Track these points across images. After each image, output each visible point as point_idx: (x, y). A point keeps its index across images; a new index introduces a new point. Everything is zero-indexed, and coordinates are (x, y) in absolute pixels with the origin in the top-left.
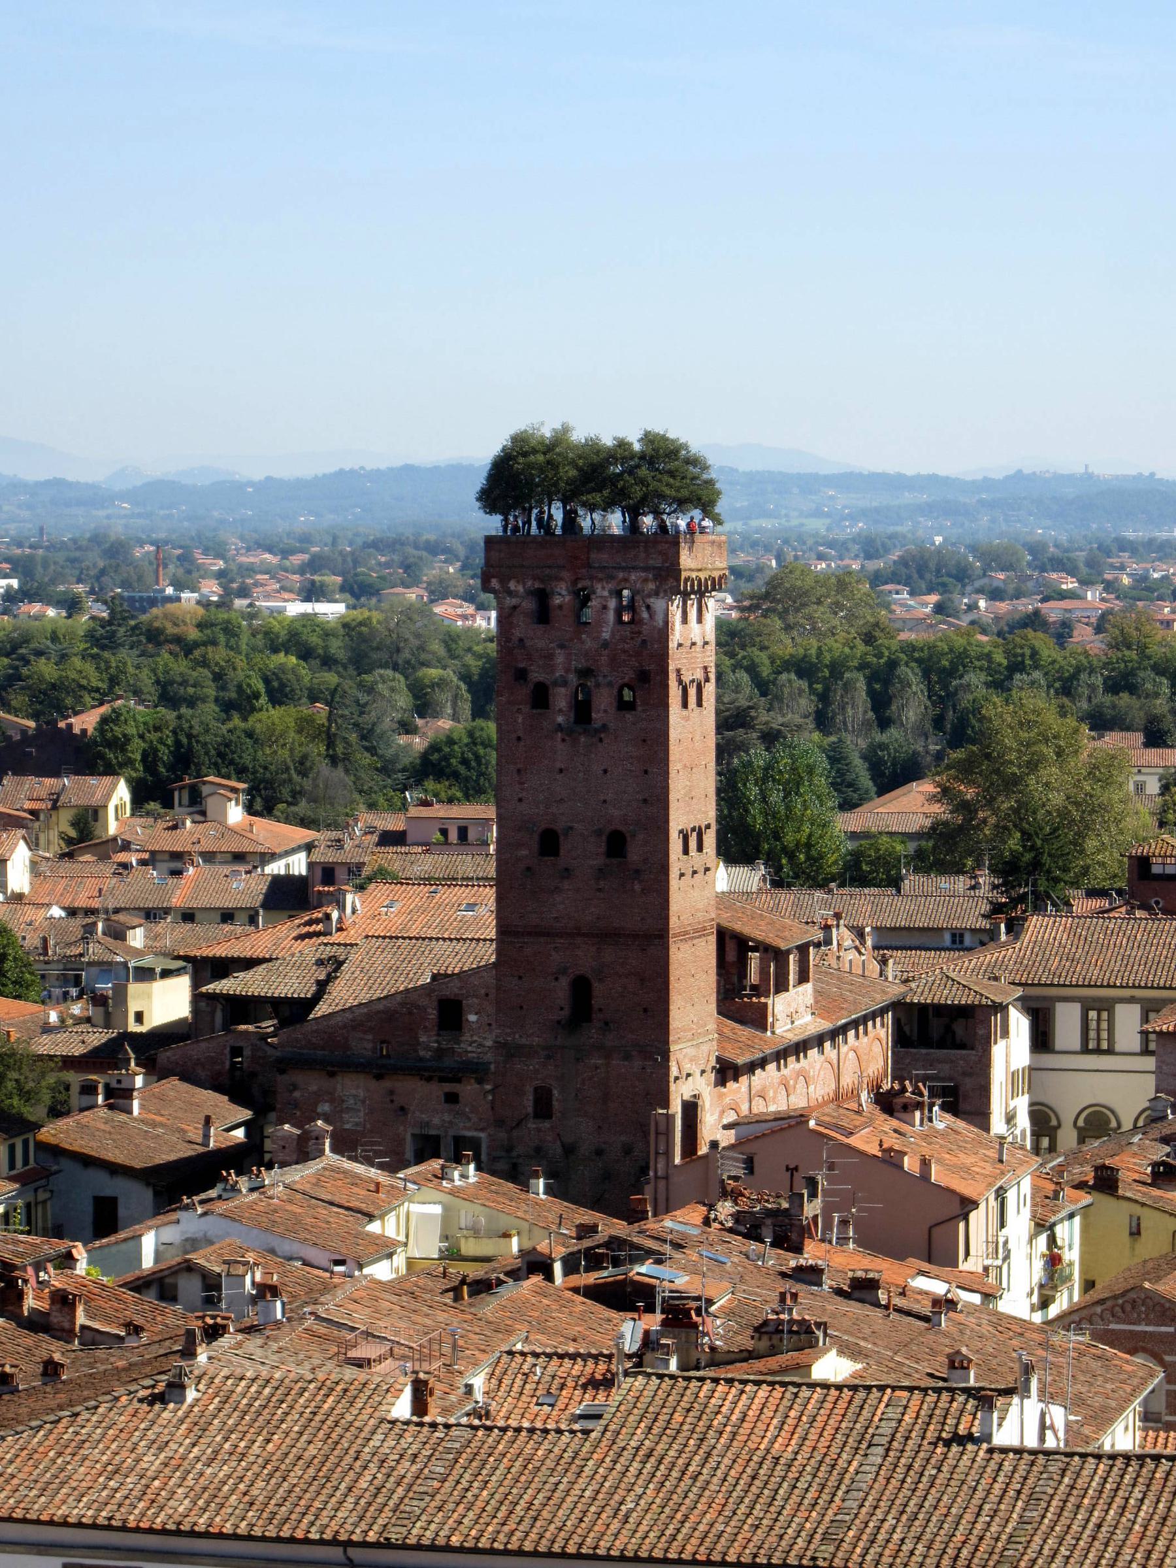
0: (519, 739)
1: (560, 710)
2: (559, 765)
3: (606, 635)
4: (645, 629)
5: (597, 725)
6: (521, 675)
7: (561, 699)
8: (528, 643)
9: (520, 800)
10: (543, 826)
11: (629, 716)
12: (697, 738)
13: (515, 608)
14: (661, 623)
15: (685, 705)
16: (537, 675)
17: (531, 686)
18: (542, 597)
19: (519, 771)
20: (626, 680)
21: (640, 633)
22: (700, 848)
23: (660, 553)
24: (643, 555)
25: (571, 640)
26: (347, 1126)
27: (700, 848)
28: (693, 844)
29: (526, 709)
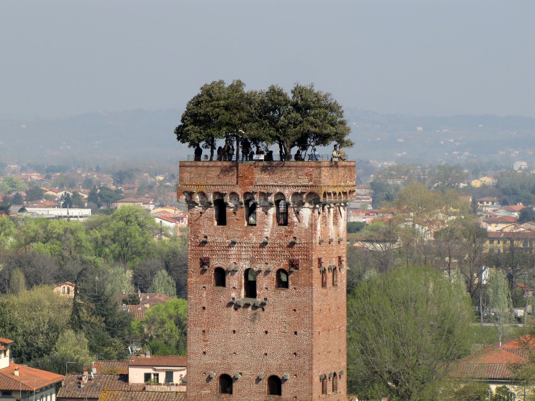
0: (204, 308)
1: (234, 288)
2: (232, 328)
3: (267, 233)
4: (296, 230)
5: (259, 300)
6: (204, 262)
7: (235, 281)
8: (209, 239)
11: (283, 293)
12: (333, 308)
13: (201, 213)
14: (307, 225)
15: (324, 285)
16: (216, 263)
18: (221, 206)
19: (204, 331)
20: (281, 267)
21: (291, 232)
22: (334, 388)
23: (306, 174)
24: (293, 176)
25: (243, 237)
27: (334, 388)
28: (329, 386)
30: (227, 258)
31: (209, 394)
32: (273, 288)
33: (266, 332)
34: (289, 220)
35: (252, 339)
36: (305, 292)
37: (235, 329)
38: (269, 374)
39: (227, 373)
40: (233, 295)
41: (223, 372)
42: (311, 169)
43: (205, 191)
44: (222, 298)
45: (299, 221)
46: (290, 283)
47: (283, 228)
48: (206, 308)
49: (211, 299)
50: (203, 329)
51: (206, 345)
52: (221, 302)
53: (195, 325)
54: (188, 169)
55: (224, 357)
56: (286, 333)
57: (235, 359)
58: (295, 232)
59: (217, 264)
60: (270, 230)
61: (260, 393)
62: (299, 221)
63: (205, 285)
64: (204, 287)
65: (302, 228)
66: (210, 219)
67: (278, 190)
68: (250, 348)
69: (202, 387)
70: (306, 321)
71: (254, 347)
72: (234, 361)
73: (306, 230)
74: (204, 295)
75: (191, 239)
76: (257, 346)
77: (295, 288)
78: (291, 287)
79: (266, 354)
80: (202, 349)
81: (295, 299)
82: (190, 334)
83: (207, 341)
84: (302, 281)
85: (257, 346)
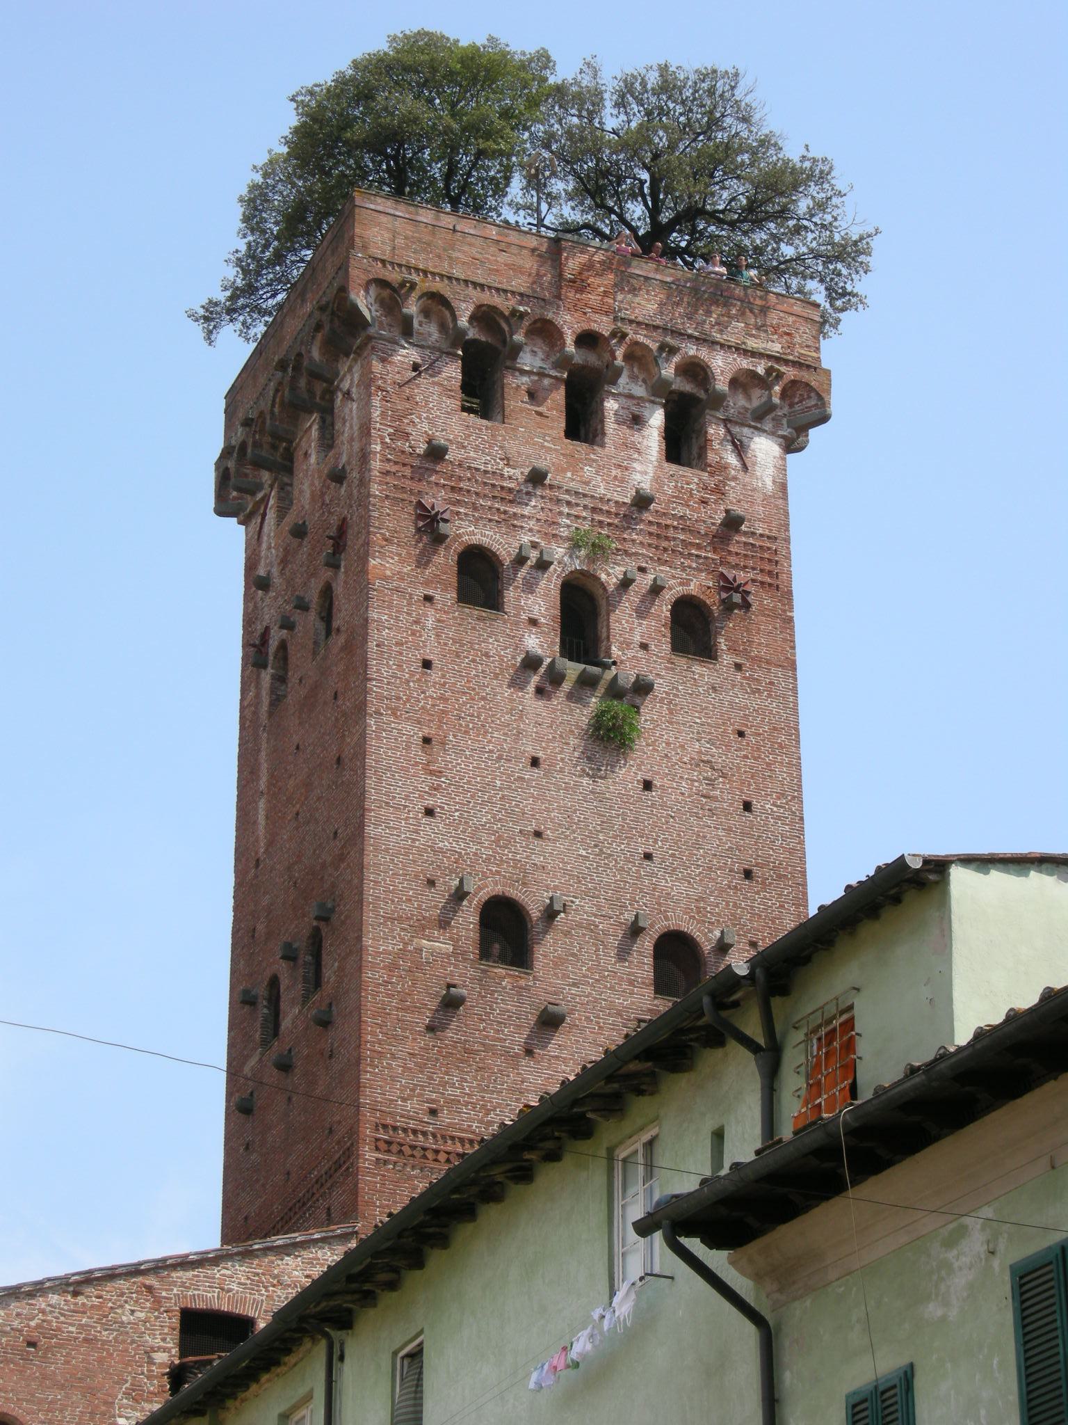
0: (427, 664)
1: (533, 622)
2: (530, 750)
4: (733, 491)
9: (429, 812)
10: (492, 888)
17: (457, 547)
19: (427, 740)
20: (693, 588)
21: (719, 491)
29: (446, 597)
30: (510, 523)
31: (449, 956)
32: (667, 647)
33: (648, 785)
34: (711, 457)
36: (771, 683)
37: (540, 754)
39: (514, 893)
40: (532, 642)
41: (499, 890)
42: (791, 319)
43: (448, 294)
44: (492, 646)
45: (745, 467)
46: (722, 643)
47: (691, 477)
49: (455, 642)
50: (426, 731)
52: (487, 655)
53: (394, 714)
54: (383, 219)
55: (500, 838)
56: (715, 799)
57: (539, 854)
58: (732, 496)
59: (473, 533)
60: (651, 470)
61: (631, 983)
62: (745, 467)
63: (431, 593)
64: (428, 599)
65: (754, 490)
66: (447, 391)
67: (691, 350)
68: (595, 822)
69: (421, 928)
70: (781, 773)
71: (606, 824)
72: (539, 860)
73: (766, 498)
74: (430, 623)
75: (382, 438)
77: (738, 667)
78: (727, 659)
79: (648, 856)
80: (421, 797)
81: (741, 699)
82: (379, 738)
83: (439, 774)
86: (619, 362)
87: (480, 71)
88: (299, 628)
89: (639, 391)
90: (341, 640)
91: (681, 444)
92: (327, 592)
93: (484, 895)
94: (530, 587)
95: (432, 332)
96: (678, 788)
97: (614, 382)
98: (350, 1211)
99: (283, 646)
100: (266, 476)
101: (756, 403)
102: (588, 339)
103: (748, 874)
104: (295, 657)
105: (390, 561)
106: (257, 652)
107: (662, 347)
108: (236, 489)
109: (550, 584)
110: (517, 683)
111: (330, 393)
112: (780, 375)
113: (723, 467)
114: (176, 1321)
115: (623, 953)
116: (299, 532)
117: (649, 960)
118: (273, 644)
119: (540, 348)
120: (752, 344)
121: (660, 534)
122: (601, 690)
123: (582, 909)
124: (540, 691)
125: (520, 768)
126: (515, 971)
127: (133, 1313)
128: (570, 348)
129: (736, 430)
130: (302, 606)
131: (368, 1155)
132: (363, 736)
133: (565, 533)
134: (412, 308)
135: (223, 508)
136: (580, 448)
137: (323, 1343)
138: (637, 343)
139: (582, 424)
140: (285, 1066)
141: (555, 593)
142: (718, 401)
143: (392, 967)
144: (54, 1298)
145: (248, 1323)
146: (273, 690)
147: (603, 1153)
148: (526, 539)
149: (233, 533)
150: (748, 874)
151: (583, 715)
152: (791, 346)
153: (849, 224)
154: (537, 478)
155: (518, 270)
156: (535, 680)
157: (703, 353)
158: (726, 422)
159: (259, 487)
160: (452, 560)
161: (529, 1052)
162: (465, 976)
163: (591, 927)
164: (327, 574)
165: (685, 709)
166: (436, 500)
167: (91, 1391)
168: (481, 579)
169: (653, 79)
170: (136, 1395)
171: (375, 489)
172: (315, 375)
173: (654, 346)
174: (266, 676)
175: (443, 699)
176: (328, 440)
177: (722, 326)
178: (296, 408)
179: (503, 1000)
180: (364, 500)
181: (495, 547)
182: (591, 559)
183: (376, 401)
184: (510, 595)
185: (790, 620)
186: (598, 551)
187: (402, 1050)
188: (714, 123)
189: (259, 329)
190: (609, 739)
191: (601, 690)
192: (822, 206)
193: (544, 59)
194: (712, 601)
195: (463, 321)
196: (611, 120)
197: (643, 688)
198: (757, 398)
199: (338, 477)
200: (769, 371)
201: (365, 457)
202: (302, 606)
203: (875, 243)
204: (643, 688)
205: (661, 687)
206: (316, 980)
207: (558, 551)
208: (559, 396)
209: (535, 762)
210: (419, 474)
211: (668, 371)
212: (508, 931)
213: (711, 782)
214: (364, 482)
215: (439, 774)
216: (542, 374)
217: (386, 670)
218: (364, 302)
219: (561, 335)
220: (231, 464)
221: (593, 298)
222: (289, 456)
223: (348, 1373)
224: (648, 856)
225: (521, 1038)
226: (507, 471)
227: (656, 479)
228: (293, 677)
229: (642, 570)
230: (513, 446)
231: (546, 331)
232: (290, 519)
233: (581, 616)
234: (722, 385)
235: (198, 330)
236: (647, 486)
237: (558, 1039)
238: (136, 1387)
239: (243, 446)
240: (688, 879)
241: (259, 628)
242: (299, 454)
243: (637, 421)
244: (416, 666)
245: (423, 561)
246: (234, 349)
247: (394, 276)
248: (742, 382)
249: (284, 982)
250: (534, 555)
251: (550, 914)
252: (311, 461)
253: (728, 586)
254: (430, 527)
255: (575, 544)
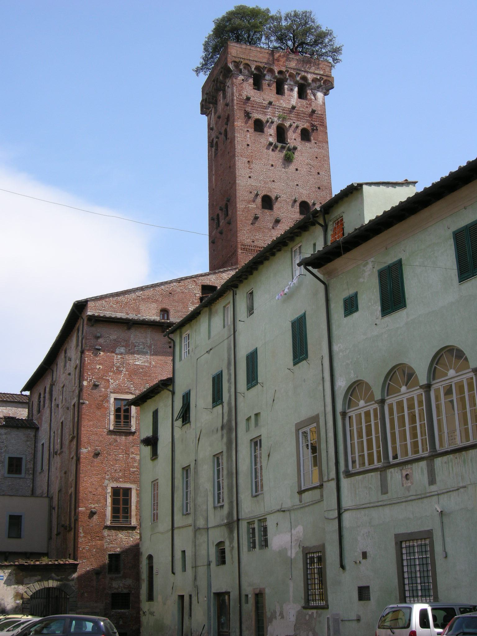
0: (248, 145)
1: (271, 135)
2: (271, 163)
9: (250, 177)
16: (256, 115)
17: (254, 119)
19: (249, 162)
20: (305, 126)
21: (310, 105)
26: (137, 363)
29: (252, 130)
30: (265, 114)
32: (300, 139)
33: (297, 170)
34: (308, 97)
35: (286, 172)
38: (300, 200)
39: (268, 194)
40: (271, 139)
41: (265, 193)
44: (262, 140)
45: (316, 99)
46: (312, 138)
47: (304, 102)
48: (250, 145)
51: (251, 172)
57: (272, 185)
62: (316, 99)
64: (248, 131)
66: (250, 85)
67: (303, 74)
69: (249, 202)
70: (326, 166)
71: (288, 178)
73: (321, 106)
74: (248, 136)
76: (291, 178)
77: (316, 143)
78: (313, 141)
79: (297, 185)
81: (316, 150)
83: (251, 169)
84: (320, 138)
85: (291, 178)
86: (287, 77)
87: (255, 13)
88: (220, 138)
89: (292, 83)
90: (229, 141)
91: (302, 95)
92: (226, 131)
93: (262, 195)
94: (270, 127)
95: (246, 72)
96: (304, 170)
97: (286, 81)
98: (236, 263)
99: (217, 142)
100: (211, 105)
101: (318, 85)
102: (280, 72)
103: (319, 188)
104: (220, 144)
105: (239, 123)
106: (212, 144)
107: (297, 73)
108: (205, 108)
109: (274, 126)
110: (268, 148)
111: (225, 86)
112: (323, 79)
113: (311, 99)
114: (200, 288)
115: (293, 206)
116: (219, 117)
117: (298, 207)
118: (215, 142)
119: (270, 75)
120: (316, 72)
121: (298, 115)
122: (286, 149)
123: (283, 197)
124: (273, 150)
125: (269, 167)
126: (270, 211)
127: (191, 286)
128: (277, 74)
129: (313, 91)
130: (221, 134)
131: (240, 251)
132: (235, 161)
133: (277, 115)
134: (242, 67)
135: (202, 113)
136: (279, 96)
137: (232, 291)
138: (291, 73)
139: (280, 91)
140: (221, 233)
141: (275, 128)
142: (309, 85)
143: (243, 211)
144: (175, 284)
145: (216, 287)
146: (215, 152)
147: (290, 250)
148: (268, 117)
149: (205, 118)
150: (319, 188)
151: (282, 155)
152: (325, 72)
153: (337, 44)
154: (270, 103)
155: (265, 57)
156: (272, 147)
157: (306, 74)
158: (311, 89)
159: (210, 108)
160: (253, 122)
161: (273, 228)
162: (259, 212)
163: (286, 201)
164: (225, 126)
165: (304, 152)
166: (249, 109)
167: (183, 303)
168: (259, 126)
169: (293, 14)
170: (193, 303)
171: (235, 107)
172: (221, 83)
173: (295, 73)
174: (213, 149)
175: (252, 152)
176: (225, 97)
177: (309, 68)
178: (217, 90)
179: (267, 217)
180: (233, 110)
181: (262, 119)
182: (283, 120)
183: (235, 88)
184: (265, 129)
185: (327, 132)
186: (284, 119)
187: (246, 229)
188: (306, 23)
189: (208, 73)
190: (288, 160)
191: (286, 149)
192: (331, 40)
193: (268, 10)
194: (310, 129)
195: (253, 69)
196: (284, 23)
197: (295, 148)
198: (318, 84)
199: (227, 105)
200: (320, 78)
201: (233, 100)
202: (221, 134)
203: (343, 48)
204: (295, 148)
205: (299, 148)
206: (227, 215)
207: (276, 119)
208: (275, 85)
209: (272, 166)
210: (245, 103)
211: (298, 79)
212: (268, 202)
213: (311, 168)
214: (233, 106)
215: (251, 169)
216: (270, 80)
217: (239, 148)
218: (231, 66)
219: (274, 71)
220: (204, 103)
221: (281, 63)
222: (216, 101)
223: (238, 297)
224: (297, 185)
225: (271, 225)
226: (264, 102)
227: (296, 103)
228: (219, 149)
229: (294, 123)
230: (265, 96)
231: (271, 71)
232: (217, 115)
233: (281, 133)
234: (310, 81)
235: (195, 73)
236: (294, 104)
237: (279, 225)
238: (193, 301)
239: (206, 99)
240: (306, 190)
241: (211, 138)
242: (218, 100)
243: (292, 90)
244: (246, 146)
245: (246, 123)
246: (203, 78)
247: (237, 60)
248: (315, 80)
249: (220, 215)
250: (270, 120)
251: (277, 198)
252: (221, 102)
253: (313, 125)
254: (248, 115)
255: (279, 118)
